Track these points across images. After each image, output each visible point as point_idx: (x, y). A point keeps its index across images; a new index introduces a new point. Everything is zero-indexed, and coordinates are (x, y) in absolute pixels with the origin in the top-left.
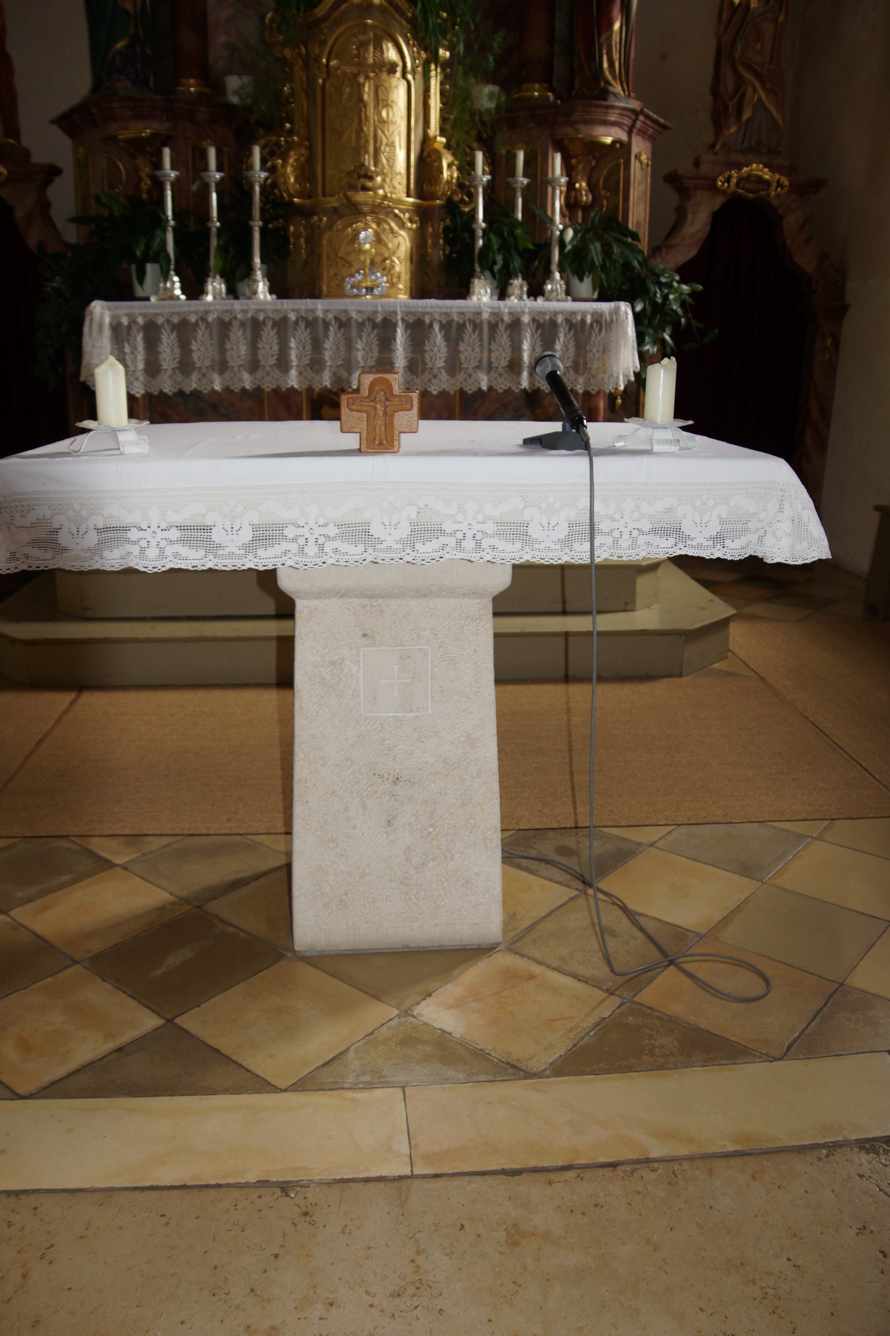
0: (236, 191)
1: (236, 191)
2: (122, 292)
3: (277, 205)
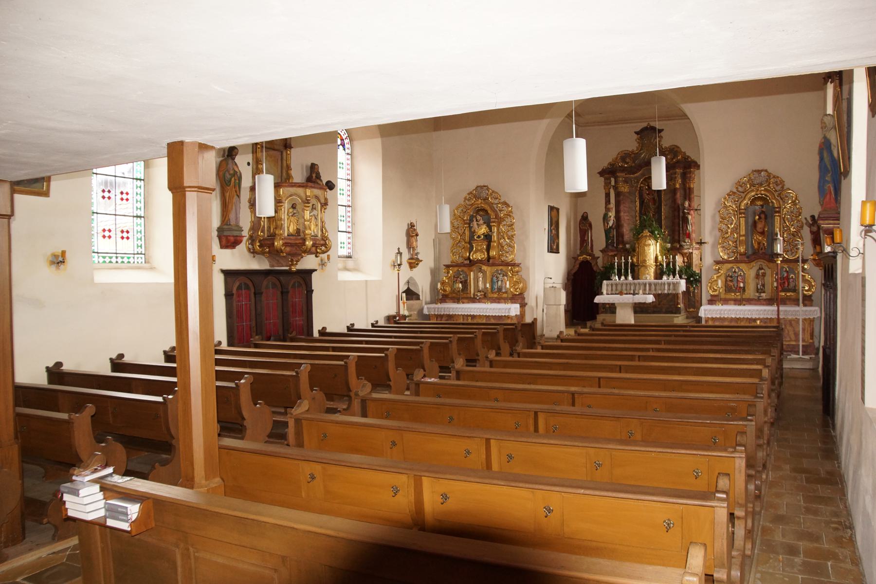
0: (626, 264)
1: (626, 264)
2: (609, 279)
3: (633, 264)
